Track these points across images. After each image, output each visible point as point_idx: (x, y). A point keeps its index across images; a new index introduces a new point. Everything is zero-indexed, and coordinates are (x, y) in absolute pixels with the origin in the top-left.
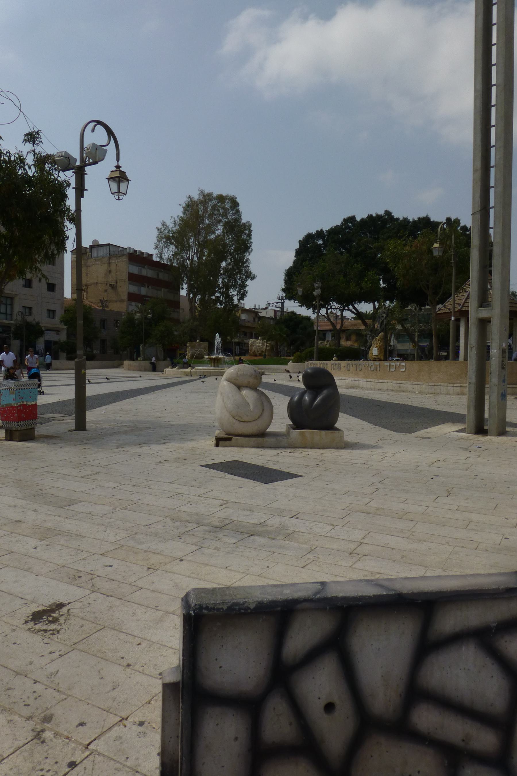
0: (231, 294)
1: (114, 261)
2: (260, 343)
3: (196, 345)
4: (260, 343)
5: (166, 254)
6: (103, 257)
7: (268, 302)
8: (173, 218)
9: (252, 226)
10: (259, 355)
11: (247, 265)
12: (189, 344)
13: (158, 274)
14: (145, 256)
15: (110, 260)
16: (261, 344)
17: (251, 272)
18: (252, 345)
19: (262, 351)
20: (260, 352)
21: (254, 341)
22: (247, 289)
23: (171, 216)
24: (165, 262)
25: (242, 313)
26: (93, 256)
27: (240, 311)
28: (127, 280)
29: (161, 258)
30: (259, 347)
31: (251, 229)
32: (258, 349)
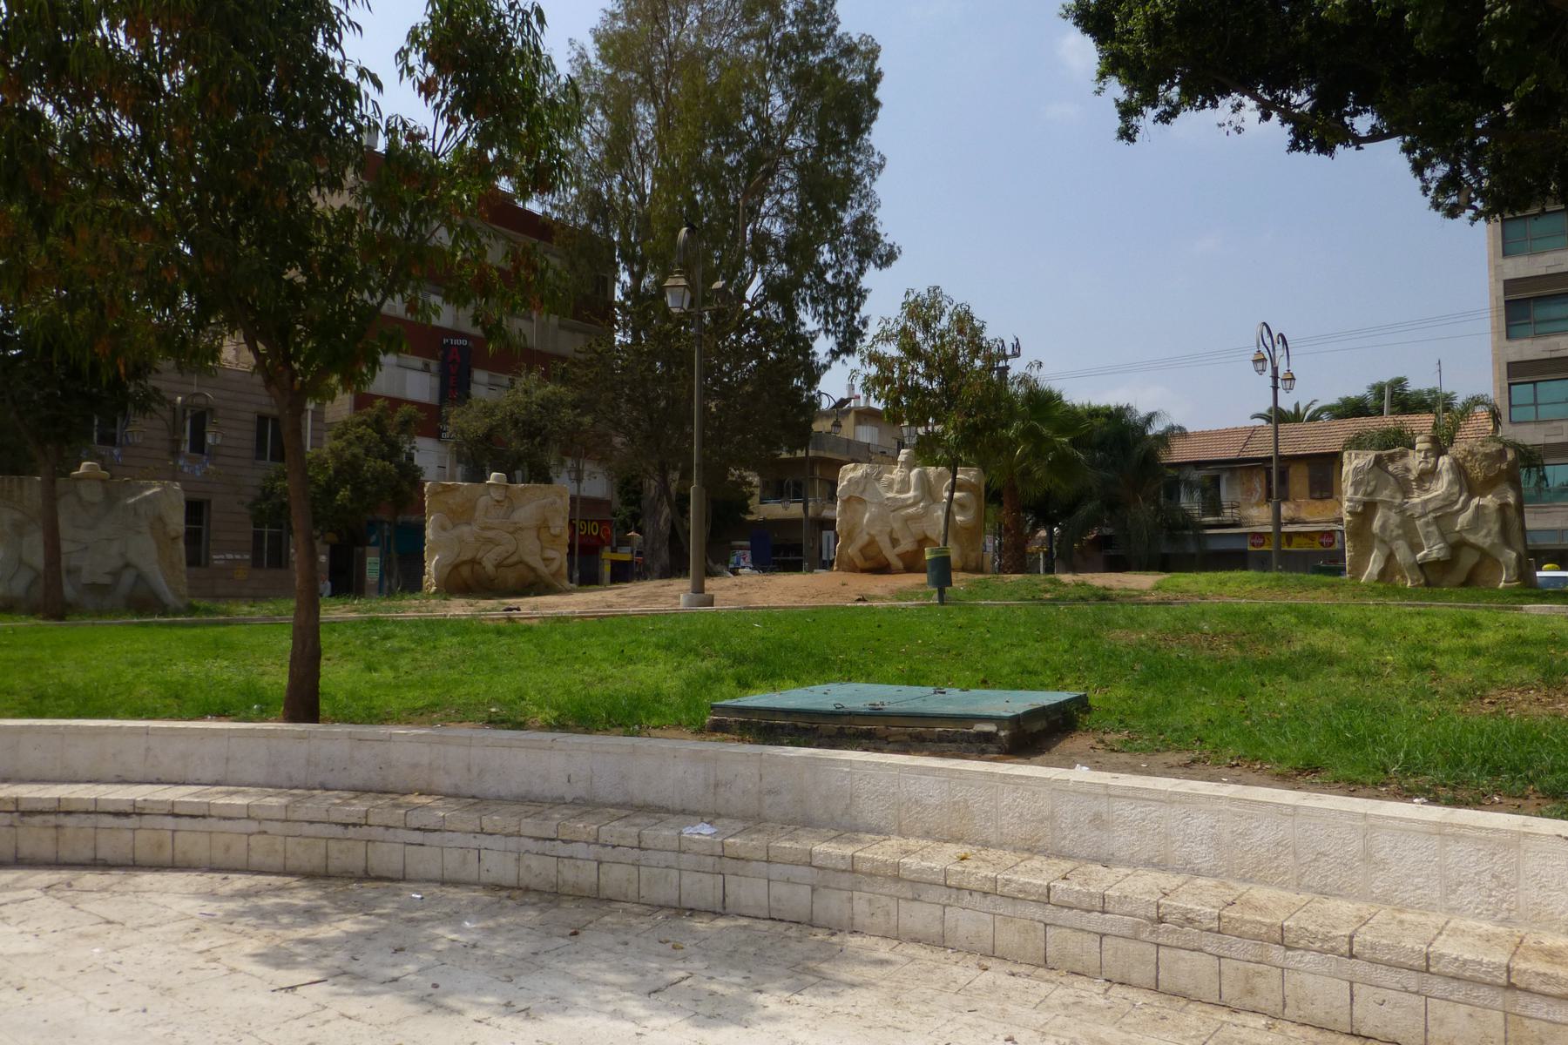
2: (905, 486)
3: (483, 501)
4: (905, 486)
8: (576, 46)
9: (881, 55)
10: (899, 564)
16: (911, 494)
19: (923, 541)
20: (907, 545)
21: (866, 476)
23: (570, 40)
25: (858, 422)
27: (852, 416)
30: (904, 512)
31: (878, 65)
32: (896, 526)
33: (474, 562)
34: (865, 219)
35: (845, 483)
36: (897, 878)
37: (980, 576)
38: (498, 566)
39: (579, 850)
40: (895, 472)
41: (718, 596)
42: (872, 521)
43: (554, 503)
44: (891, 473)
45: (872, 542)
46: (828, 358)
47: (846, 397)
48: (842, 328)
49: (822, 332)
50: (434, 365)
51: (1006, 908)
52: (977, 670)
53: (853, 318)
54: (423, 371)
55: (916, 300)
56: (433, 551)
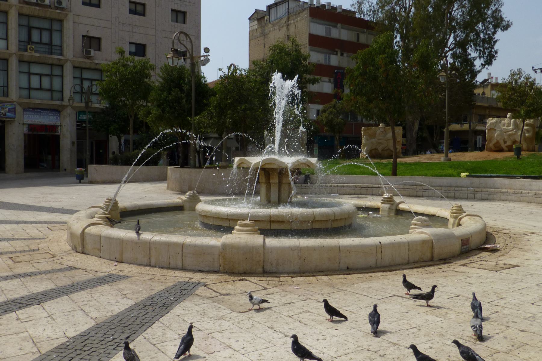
0: (469, 57)
1: (293, 21)
2: (509, 125)
3: (378, 132)
5: (367, 4)
6: (281, 18)
7: (533, 68)
10: (507, 149)
11: (497, 9)
12: (365, 130)
13: (358, 36)
14: (338, 10)
15: (288, 21)
16: (511, 127)
17: (503, 16)
18: (492, 130)
19: (515, 142)
20: (509, 143)
21: (496, 122)
22: (496, 47)
24: (367, 18)
25: (492, 89)
26: (271, 21)
27: (489, 87)
28: (308, 45)
29: (361, 11)
30: (508, 133)
32: (505, 137)
33: (376, 149)
34: (497, 11)
35: (489, 124)
36: (501, 192)
37: (533, 153)
38: (382, 150)
39: (451, 191)
40: (506, 120)
41: (452, 158)
42: (498, 135)
43: (398, 132)
44: (504, 121)
45: (498, 142)
46: (480, 68)
47: (487, 78)
48: (486, 55)
49: (478, 58)
50: (332, 80)
51: (516, 195)
52: (521, 172)
53: (491, 51)
54: (328, 82)
55: (513, 72)
56: (364, 146)
